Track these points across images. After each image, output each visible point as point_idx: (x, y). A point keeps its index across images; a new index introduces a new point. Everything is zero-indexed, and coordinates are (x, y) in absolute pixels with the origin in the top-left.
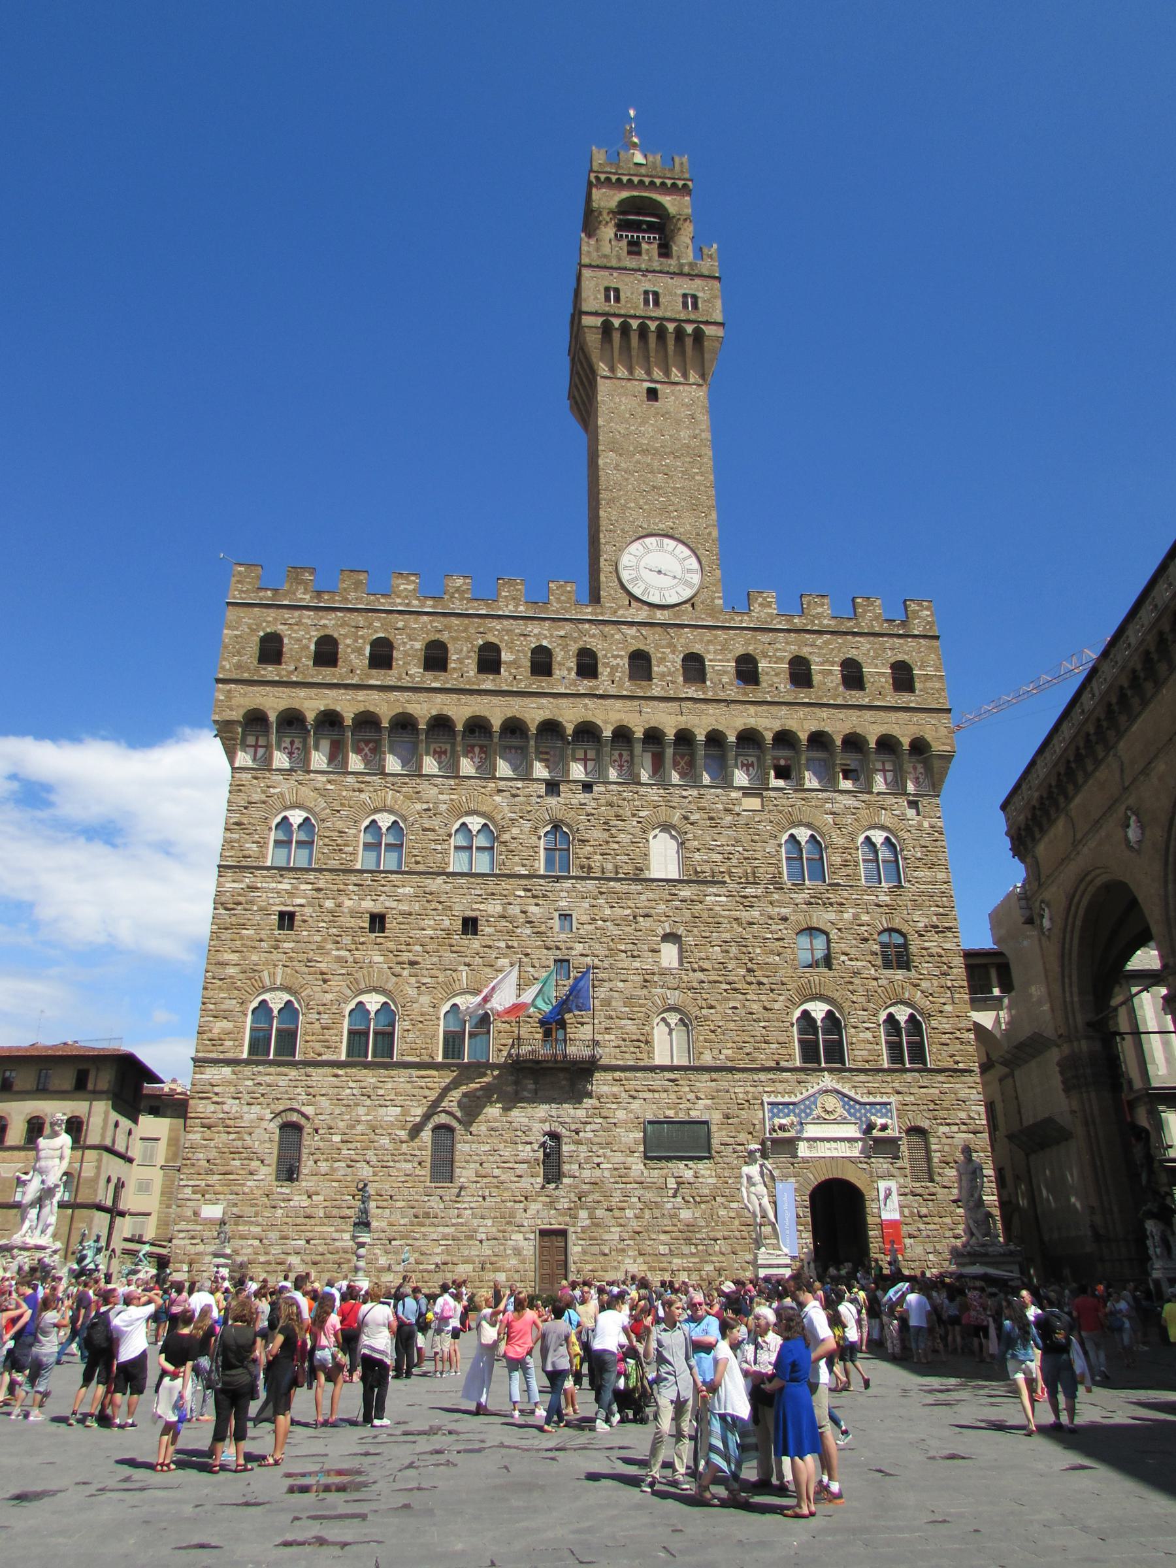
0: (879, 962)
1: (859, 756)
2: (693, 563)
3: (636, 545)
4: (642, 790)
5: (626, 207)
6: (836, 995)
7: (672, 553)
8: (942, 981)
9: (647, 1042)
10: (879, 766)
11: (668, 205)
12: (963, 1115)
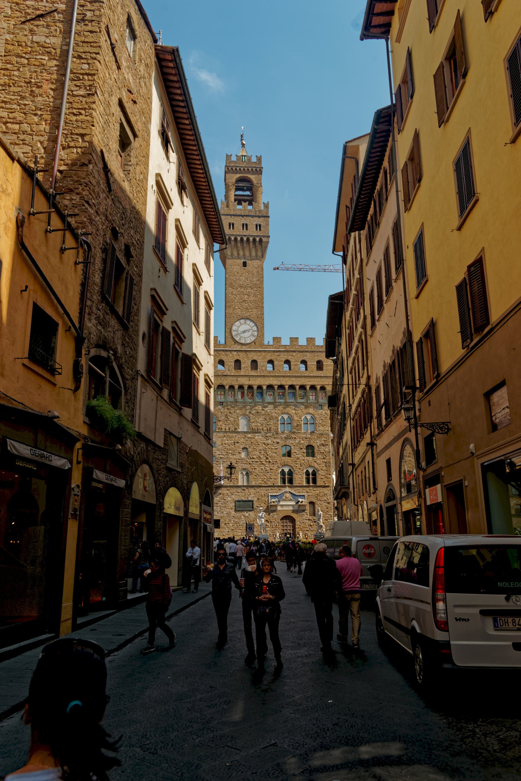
0: (305, 455)
1: (305, 391)
2: (255, 328)
3: (238, 322)
4: (238, 404)
5: (239, 180)
6: (292, 465)
7: (249, 325)
8: (324, 460)
9: (237, 479)
10: (311, 394)
11: (253, 180)
12: (326, 498)
